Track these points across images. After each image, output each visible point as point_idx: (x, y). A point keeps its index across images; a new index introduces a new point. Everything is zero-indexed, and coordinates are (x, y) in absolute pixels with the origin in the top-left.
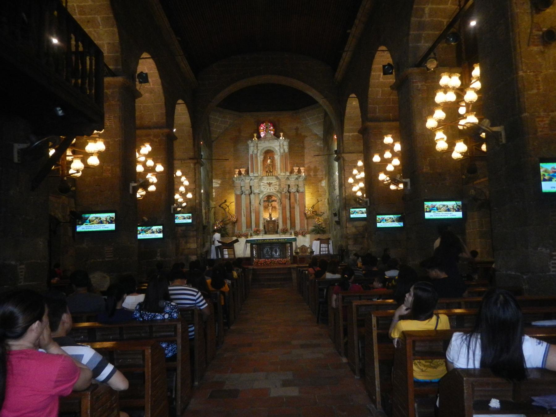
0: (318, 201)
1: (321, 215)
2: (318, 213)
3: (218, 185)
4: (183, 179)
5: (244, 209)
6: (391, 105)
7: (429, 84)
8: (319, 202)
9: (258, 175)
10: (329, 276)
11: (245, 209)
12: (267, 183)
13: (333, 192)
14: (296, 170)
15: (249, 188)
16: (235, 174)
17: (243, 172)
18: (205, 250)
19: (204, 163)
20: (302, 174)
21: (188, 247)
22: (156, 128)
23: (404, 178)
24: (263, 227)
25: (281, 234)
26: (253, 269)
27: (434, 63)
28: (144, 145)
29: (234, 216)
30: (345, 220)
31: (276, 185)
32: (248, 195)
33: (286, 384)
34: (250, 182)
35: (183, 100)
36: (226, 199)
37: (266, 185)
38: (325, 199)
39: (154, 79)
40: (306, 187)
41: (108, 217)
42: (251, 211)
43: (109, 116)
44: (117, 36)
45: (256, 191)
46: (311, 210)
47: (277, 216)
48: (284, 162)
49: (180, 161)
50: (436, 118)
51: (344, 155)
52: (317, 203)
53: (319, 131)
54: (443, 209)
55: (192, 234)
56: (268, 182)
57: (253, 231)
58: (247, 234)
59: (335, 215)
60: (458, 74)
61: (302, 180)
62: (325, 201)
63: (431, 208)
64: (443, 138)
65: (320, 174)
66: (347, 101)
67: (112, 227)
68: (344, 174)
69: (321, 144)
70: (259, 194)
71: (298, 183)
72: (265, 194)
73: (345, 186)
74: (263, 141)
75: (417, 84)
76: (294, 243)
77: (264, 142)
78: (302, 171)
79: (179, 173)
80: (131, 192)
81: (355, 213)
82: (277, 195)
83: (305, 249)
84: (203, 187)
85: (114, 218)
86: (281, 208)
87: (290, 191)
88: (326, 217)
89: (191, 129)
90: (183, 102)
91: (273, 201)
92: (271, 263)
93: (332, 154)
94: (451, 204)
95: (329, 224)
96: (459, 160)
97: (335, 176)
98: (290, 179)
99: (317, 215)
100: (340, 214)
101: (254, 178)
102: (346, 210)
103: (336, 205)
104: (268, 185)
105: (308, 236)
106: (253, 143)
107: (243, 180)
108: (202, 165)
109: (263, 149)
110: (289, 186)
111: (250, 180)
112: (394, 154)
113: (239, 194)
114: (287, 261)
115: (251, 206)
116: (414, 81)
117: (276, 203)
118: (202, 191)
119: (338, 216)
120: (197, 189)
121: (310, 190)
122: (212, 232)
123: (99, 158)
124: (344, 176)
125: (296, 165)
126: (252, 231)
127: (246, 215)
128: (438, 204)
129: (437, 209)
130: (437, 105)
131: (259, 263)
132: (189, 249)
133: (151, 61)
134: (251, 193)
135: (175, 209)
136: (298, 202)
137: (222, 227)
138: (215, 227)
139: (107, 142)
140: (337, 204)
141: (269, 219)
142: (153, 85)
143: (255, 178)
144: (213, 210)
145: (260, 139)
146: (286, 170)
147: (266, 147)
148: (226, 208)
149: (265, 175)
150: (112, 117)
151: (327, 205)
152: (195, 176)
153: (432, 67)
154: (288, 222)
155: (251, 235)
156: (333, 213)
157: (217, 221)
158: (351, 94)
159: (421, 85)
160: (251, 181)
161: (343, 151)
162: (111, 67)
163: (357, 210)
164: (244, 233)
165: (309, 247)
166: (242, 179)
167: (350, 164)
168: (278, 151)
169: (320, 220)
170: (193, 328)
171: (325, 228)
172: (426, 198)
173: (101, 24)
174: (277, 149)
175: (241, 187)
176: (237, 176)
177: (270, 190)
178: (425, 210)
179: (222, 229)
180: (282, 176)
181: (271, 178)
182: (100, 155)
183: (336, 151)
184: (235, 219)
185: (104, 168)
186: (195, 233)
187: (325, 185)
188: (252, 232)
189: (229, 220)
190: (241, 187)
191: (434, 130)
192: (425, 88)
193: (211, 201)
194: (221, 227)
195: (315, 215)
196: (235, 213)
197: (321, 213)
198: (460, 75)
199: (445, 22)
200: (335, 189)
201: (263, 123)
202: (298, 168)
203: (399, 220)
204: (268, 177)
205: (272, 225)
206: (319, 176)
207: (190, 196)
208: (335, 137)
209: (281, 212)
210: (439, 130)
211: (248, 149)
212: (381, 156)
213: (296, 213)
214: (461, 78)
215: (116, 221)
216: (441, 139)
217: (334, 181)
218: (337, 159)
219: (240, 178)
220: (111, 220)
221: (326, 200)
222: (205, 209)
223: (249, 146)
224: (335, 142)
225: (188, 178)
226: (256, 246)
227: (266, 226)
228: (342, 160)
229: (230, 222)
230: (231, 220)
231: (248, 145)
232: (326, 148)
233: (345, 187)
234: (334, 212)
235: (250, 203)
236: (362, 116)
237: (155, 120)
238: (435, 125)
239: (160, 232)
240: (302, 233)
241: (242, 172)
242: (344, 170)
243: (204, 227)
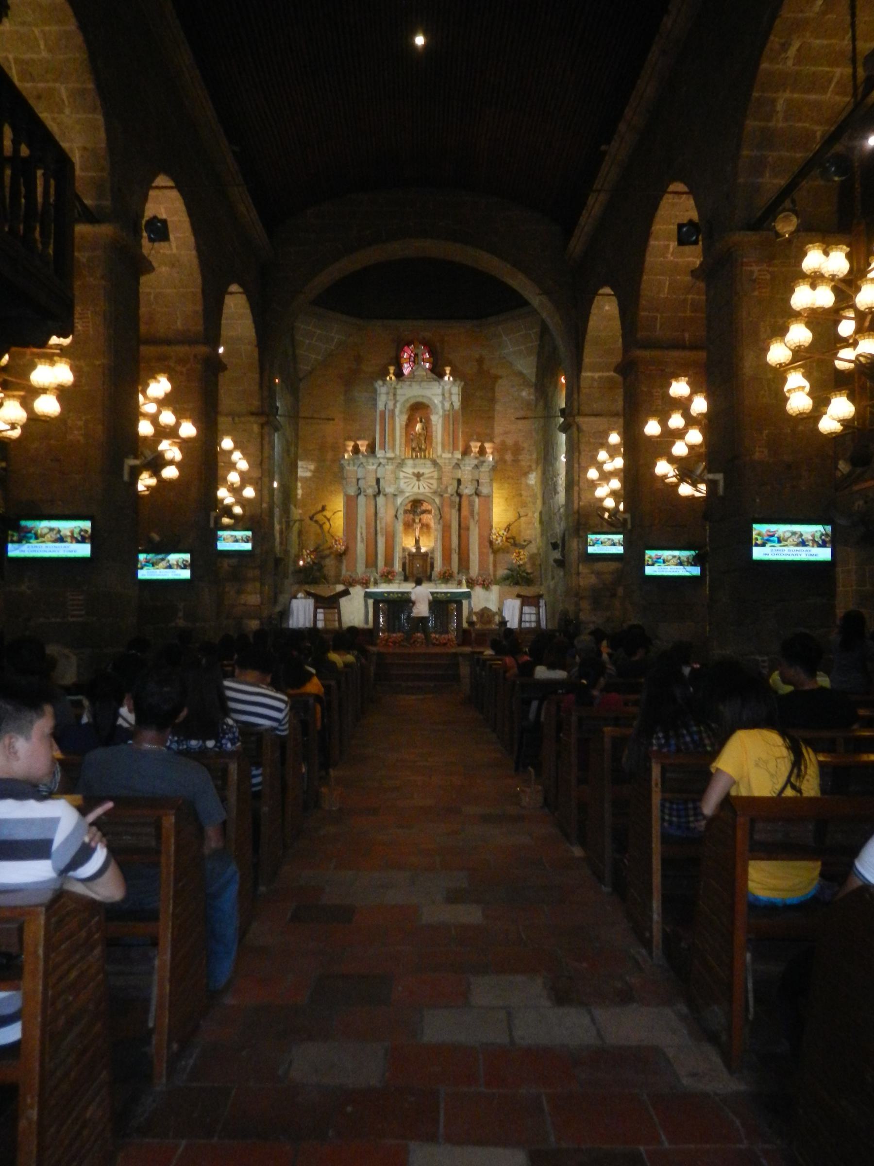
0: (520, 517)
1: (523, 545)
2: (517, 542)
3: (309, 474)
4: (237, 456)
5: (361, 528)
6: (688, 314)
7: (776, 269)
8: (522, 518)
9: (396, 455)
10: (542, 672)
11: (364, 526)
12: (414, 474)
13: (552, 498)
14: (476, 447)
15: (374, 483)
16: (346, 451)
17: (363, 449)
18: (278, 609)
19: (281, 426)
20: (489, 456)
21: (242, 602)
22: (181, 342)
23: (709, 472)
24: (401, 565)
25: (437, 582)
26: (379, 654)
27: (792, 221)
28: (155, 378)
29: (341, 541)
30: (577, 559)
31: (432, 478)
32: (372, 498)
33: (454, 897)
34: (377, 469)
35: (241, 285)
36: (324, 504)
37: (410, 478)
38: (534, 512)
39: (181, 235)
40: (495, 486)
41: (75, 530)
42: (376, 531)
43: (82, 310)
44: (102, 135)
45: (390, 489)
46: (503, 534)
47: (432, 544)
48: (451, 429)
49: (230, 419)
50: (792, 343)
51: (580, 420)
52: (516, 520)
53: (527, 366)
54: (790, 542)
55: (251, 574)
56: (416, 471)
57: (379, 574)
58: (366, 580)
59: (555, 546)
60: (845, 247)
61: (487, 470)
62: (534, 517)
63: (766, 538)
64: (803, 388)
65: (526, 459)
66: (591, 302)
67: (84, 550)
68: (579, 459)
69: (529, 394)
70: (395, 495)
71: (479, 475)
72: (408, 497)
73: (578, 485)
74: (408, 383)
75: (749, 268)
76: (465, 603)
77: (410, 385)
78: (489, 451)
79: (227, 443)
80: (126, 477)
81: (599, 544)
83: (488, 616)
84: (276, 477)
85: (90, 531)
86: (439, 527)
87: (461, 494)
88: (535, 551)
89: (257, 349)
90: (241, 290)
91: (424, 512)
92: (416, 643)
93: (555, 417)
94: (809, 530)
95: (540, 565)
96: (834, 438)
97: (557, 463)
98: (461, 466)
99: (515, 545)
100: (566, 548)
101: (386, 461)
102: (579, 536)
103: (557, 526)
104: (416, 478)
105: (495, 589)
106: (387, 386)
107: (362, 465)
108: (276, 429)
109: (407, 400)
110: (459, 481)
111: (378, 464)
112: (690, 421)
113: (353, 494)
114: (449, 640)
115: (378, 522)
116: (745, 260)
117: (430, 516)
118: (275, 485)
119: (560, 549)
120: (266, 480)
121: (503, 491)
122: (293, 573)
123: (60, 399)
124: (579, 464)
125: (475, 437)
126: (377, 573)
127: (367, 541)
128: (782, 529)
129: (779, 541)
130: (796, 315)
131: (390, 640)
132: (245, 605)
133: (174, 194)
134: (379, 493)
135: (218, 520)
136: (476, 517)
137: (314, 563)
138: (301, 563)
139: (77, 366)
140: (560, 524)
141: (414, 550)
142: (177, 248)
144: (296, 528)
145: (401, 379)
146: (455, 447)
147: (415, 396)
148: (325, 523)
149: (410, 457)
150: (89, 312)
151: (537, 525)
152: (262, 452)
153: (785, 231)
154: (455, 557)
155: (376, 583)
156: (551, 543)
157: (304, 551)
158: (602, 287)
159: (759, 271)
160: (379, 469)
161: (579, 410)
162: (88, 202)
163: (603, 537)
164: (360, 578)
165: (497, 613)
166: (360, 462)
167: (592, 440)
168: (440, 406)
169: (522, 557)
170: (259, 772)
171: (531, 573)
172: (756, 516)
173: (66, 102)
174: (436, 401)
175: (358, 480)
176: (350, 455)
177: (419, 488)
178: (754, 542)
179: (315, 568)
180: (445, 459)
181: (422, 464)
182: (62, 393)
183: (563, 412)
184: (343, 547)
185: (69, 422)
186: (257, 572)
187: (536, 482)
188: (378, 576)
189: (330, 548)
190: (358, 480)
191: (785, 368)
192: (768, 277)
193: (292, 507)
194: (311, 563)
195: (511, 545)
196: (344, 534)
197: (525, 541)
198: (848, 249)
199: (820, 131)
200: (556, 492)
201: (408, 345)
202: (479, 444)
203: (694, 562)
205: (421, 563)
206: (523, 463)
207: (249, 492)
208: (563, 380)
209: (439, 537)
210: (795, 368)
211: (375, 400)
212: (663, 423)
213: (471, 540)
214: (849, 256)
215: (93, 538)
216: (799, 388)
217: (556, 475)
218: (565, 428)
219: (356, 461)
220: (82, 537)
221: (537, 515)
222: (280, 523)
223: (378, 392)
224: (562, 391)
225: (246, 455)
226: (386, 606)
227: (407, 565)
228: (574, 429)
229: (331, 553)
230: (334, 549)
231: (375, 391)
232: (541, 403)
233: (579, 488)
234: (553, 541)
235: (376, 514)
236: (624, 336)
237: (179, 325)
238: (787, 358)
239: (185, 567)
240: (484, 581)
241: (360, 448)
242: (580, 453)
243: (278, 561)
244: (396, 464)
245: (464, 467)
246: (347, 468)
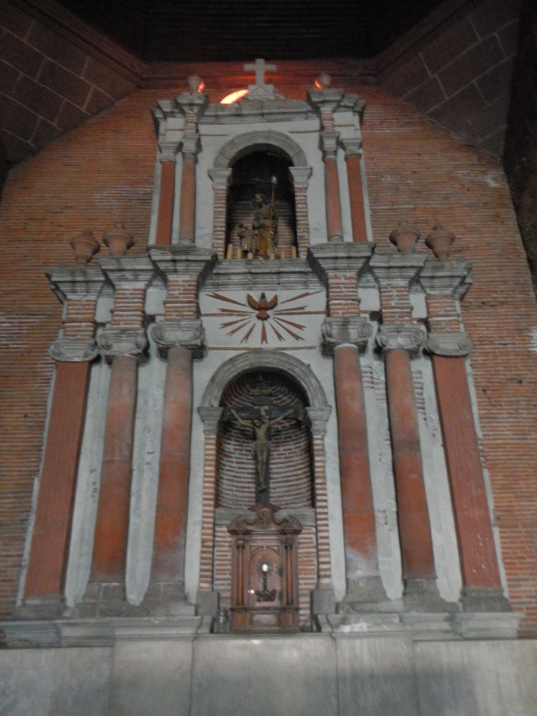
61: (449, 292)
72: (232, 360)
82: (302, 364)
87: (388, 347)
113: (76, 360)
143: (174, 261)
177: (264, 338)
204: (255, 262)
244: (200, 267)
245: (388, 278)
246: (70, 296)
